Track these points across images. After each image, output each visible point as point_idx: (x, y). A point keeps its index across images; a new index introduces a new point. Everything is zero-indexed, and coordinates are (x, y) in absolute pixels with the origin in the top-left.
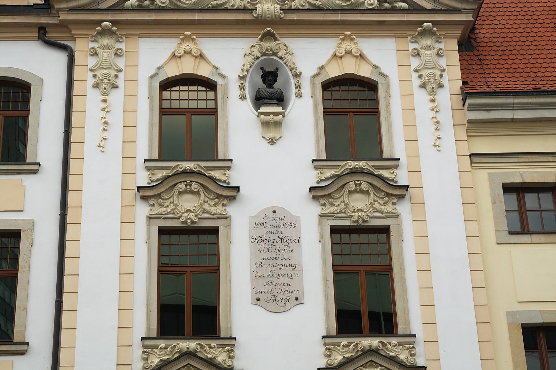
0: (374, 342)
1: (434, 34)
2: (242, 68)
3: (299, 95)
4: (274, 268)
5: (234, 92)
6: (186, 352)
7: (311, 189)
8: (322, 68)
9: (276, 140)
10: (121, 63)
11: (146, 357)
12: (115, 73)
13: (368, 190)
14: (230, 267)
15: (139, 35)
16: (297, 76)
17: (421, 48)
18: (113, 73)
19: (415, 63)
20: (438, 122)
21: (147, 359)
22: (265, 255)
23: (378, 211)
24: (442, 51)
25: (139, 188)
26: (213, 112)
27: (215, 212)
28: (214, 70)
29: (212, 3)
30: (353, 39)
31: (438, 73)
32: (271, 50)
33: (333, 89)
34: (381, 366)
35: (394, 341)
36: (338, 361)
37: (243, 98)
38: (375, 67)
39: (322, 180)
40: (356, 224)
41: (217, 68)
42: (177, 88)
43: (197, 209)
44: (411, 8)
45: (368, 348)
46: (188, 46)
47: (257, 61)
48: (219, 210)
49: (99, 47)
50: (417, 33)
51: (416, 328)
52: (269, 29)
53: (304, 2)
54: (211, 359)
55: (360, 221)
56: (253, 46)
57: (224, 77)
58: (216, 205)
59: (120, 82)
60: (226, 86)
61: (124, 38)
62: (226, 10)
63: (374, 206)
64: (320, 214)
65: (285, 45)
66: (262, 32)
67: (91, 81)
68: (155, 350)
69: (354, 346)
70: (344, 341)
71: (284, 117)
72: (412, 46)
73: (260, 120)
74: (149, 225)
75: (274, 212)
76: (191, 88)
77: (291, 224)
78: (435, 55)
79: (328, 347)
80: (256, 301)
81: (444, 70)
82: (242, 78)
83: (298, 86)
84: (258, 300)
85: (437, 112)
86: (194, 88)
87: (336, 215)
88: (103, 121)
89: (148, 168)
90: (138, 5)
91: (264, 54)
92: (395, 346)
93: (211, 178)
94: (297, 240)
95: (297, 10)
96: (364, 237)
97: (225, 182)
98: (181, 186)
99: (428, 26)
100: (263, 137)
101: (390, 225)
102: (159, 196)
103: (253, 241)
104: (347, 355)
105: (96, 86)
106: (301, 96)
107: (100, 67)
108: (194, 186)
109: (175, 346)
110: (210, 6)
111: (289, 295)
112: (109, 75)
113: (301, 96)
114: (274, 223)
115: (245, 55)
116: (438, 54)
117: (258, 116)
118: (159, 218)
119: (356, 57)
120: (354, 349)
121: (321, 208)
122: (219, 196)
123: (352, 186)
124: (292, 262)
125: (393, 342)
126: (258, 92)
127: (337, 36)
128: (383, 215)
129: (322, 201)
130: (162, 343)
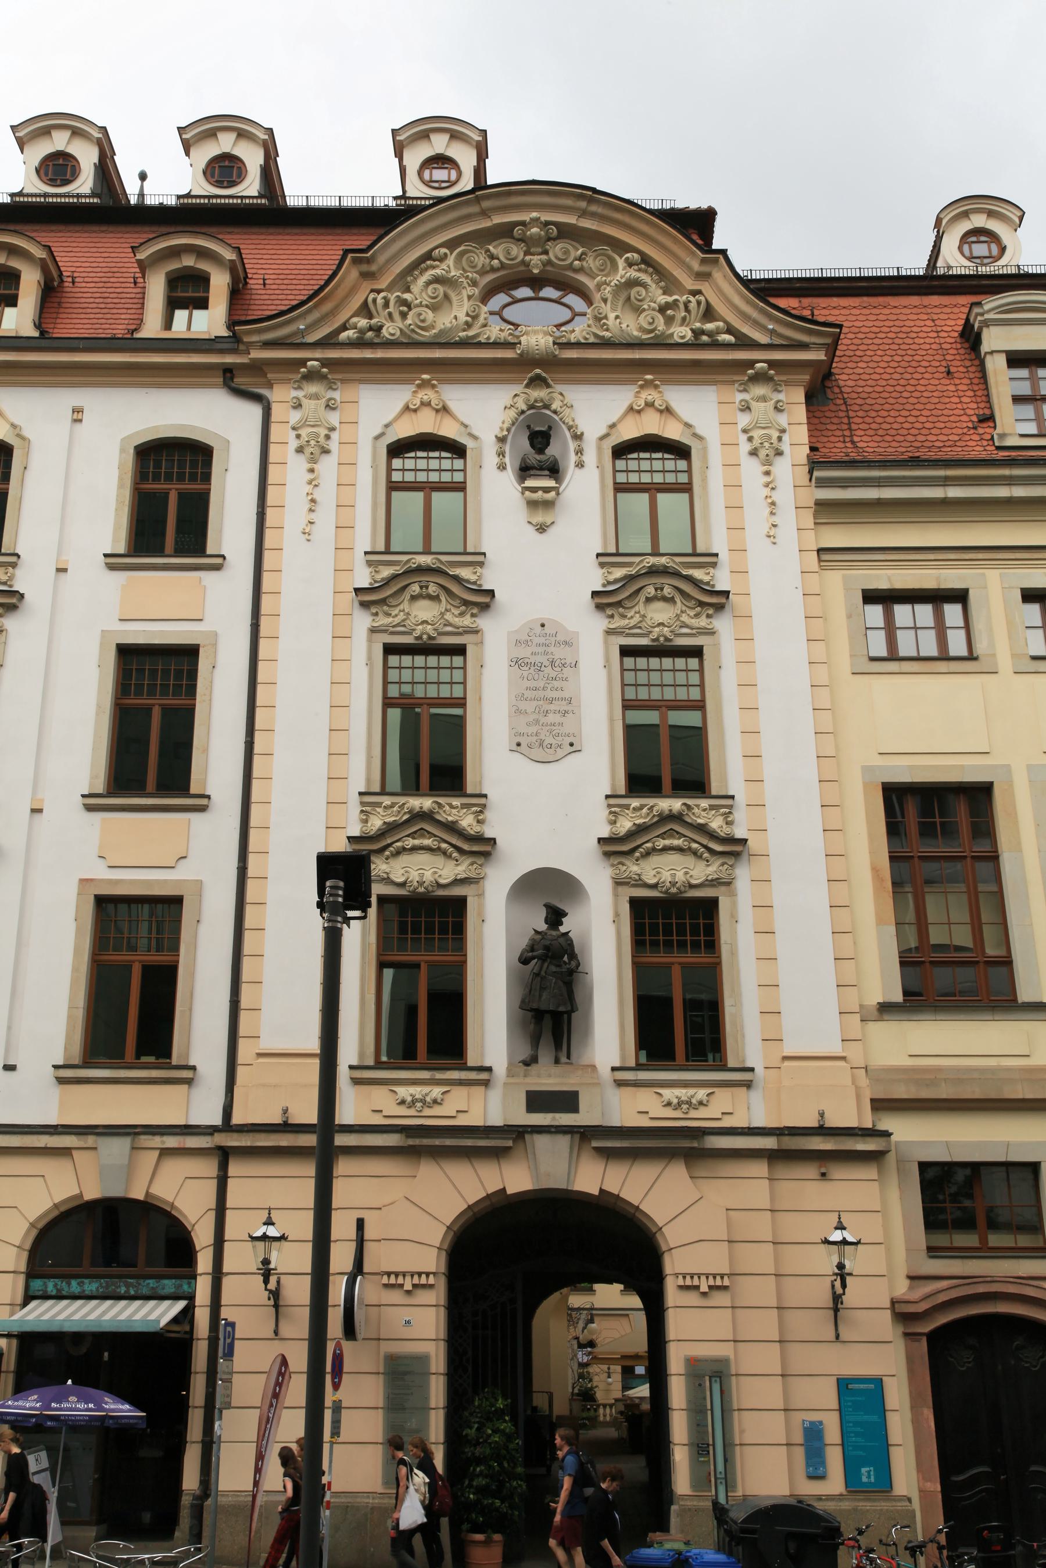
0: (676, 804)
1: (770, 379)
2: (501, 425)
3: (580, 465)
4: (541, 702)
5: (490, 459)
6: (418, 812)
7: (595, 594)
8: (613, 426)
9: (547, 527)
10: (334, 418)
11: (364, 817)
12: (326, 432)
13: (673, 597)
14: (480, 699)
15: (360, 380)
16: (578, 437)
17: (752, 399)
18: (323, 432)
19: (744, 420)
20: (773, 504)
21: (366, 821)
22: (529, 684)
23: (687, 626)
24: (781, 404)
25: (357, 591)
27: (461, 624)
28: (463, 429)
29: (460, 334)
30: (656, 387)
31: (775, 434)
32: (542, 401)
33: (629, 456)
34: (685, 836)
35: (704, 803)
36: (627, 829)
37: (502, 467)
38: (688, 425)
39: (609, 583)
40: (655, 644)
41: (466, 426)
42: (412, 454)
43: (436, 620)
44: (739, 343)
45: (667, 812)
46: (427, 395)
47: (522, 417)
48: (467, 621)
49: (305, 396)
50: (747, 378)
51: (736, 785)
52: (538, 371)
53: (588, 333)
54: (453, 822)
55: (662, 639)
56: (516, 395)
57: (475, 438)
58: (462, 614)
59: (334, 445)
60: (479, 451)
61: (339, 384)
62: (480, 345)
63: (682, 619)
64: (605, 628)
65: (561, 394)
66: (530, 375)
67: (294, 443)
68: (378, 809)
69: (649, 809)
70: (635, 803)
71: (558, 494)
72: (740, 396)
73: (525, 499)
74: (370, 640)
75: (543, 625)
77: (566, 643)
78: (772, 408)
79: (613, 809)
80: (515, 747)
81: (783, 431)
82: (502, 440)
83: (579, 452)
84: (519, 745)
85: (773, 489)
86: (436, 454)
87: (627, 631)
88: (310, 498)
89: (369, 563)
90: (358, 338)
91: (531, 407)
92: (704, 810)
93: (457, 579)
94: (573, 665)
95: (578, 345)
96: (667, 662)
97: (475, 583)
98: (414, 588)
99: (762, 368)
100: (529, 522)
101: (702, 646)
102: (383, 602)
103: (513, 664)
104: (638, 822)
105: (300, 450)
106: (582, 466)
107: (304, 423)
108: (432, 589)
109: (404, 804)
110: (457, 339)
111: (560, 738)
112: (317, 435)
113: (582, 466)
114: (542, 640)
115: (505, 408)
116: (776, 408)
117: (523, 493)
118: (385, 631)
119: (661, 412)
120: (648, 814)
121: (607, 620)
123: (651, 591)
124: (566, 694)
125: (702, 805)
126: (523, 460)
127: (633, 382)
128: (694, 631)
129: (609, 612)
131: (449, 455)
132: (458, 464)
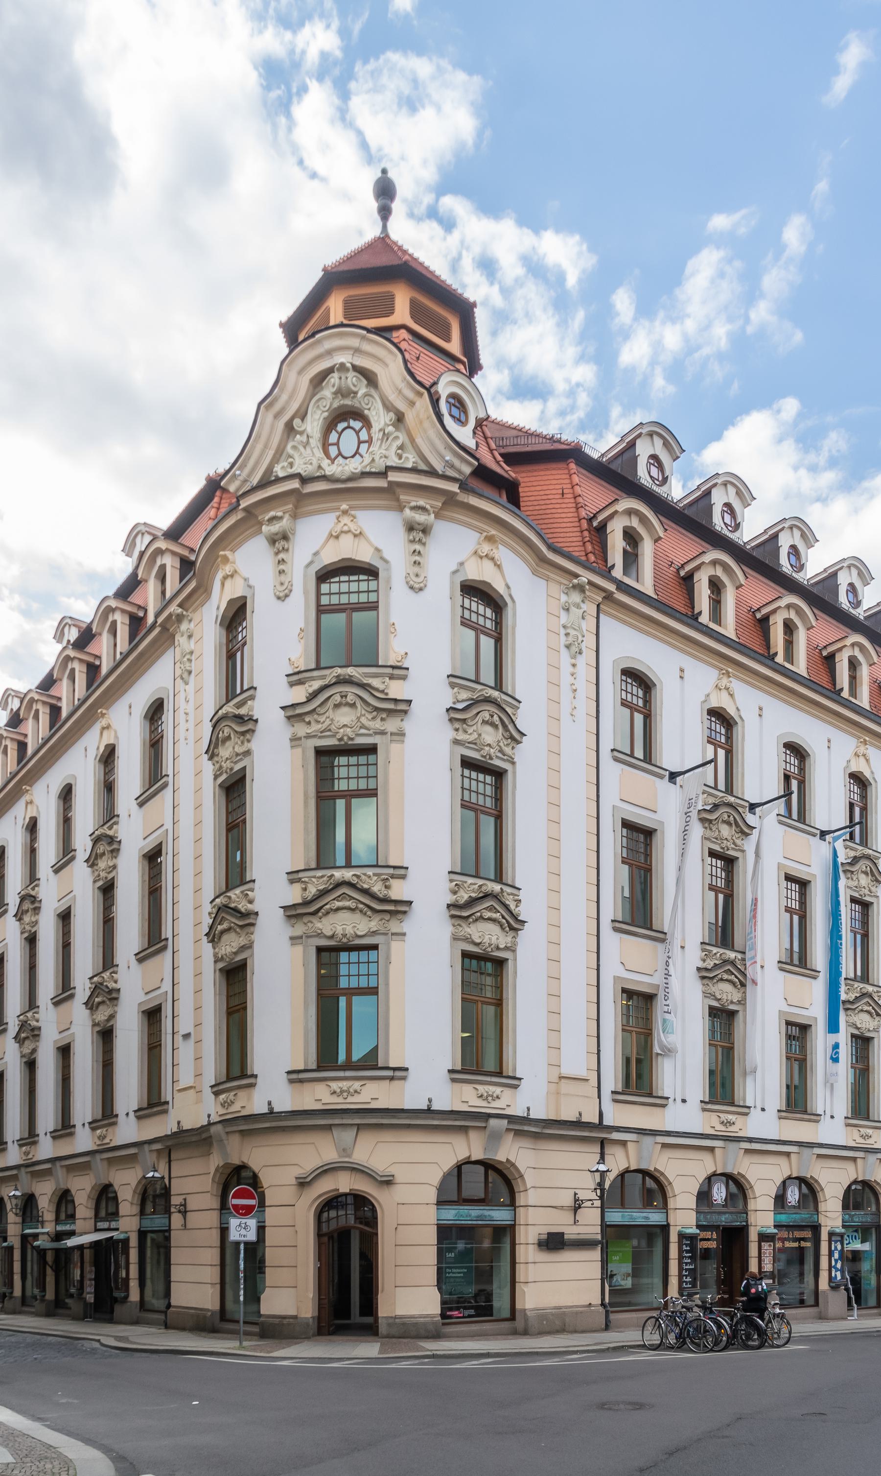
11: (304, 886)
26: (373, 607)
58: (374, 718)
76: (353, 578)
122: (377, 709)
130: (319, 873)
131: (365, 577)
132: (373, 585)
